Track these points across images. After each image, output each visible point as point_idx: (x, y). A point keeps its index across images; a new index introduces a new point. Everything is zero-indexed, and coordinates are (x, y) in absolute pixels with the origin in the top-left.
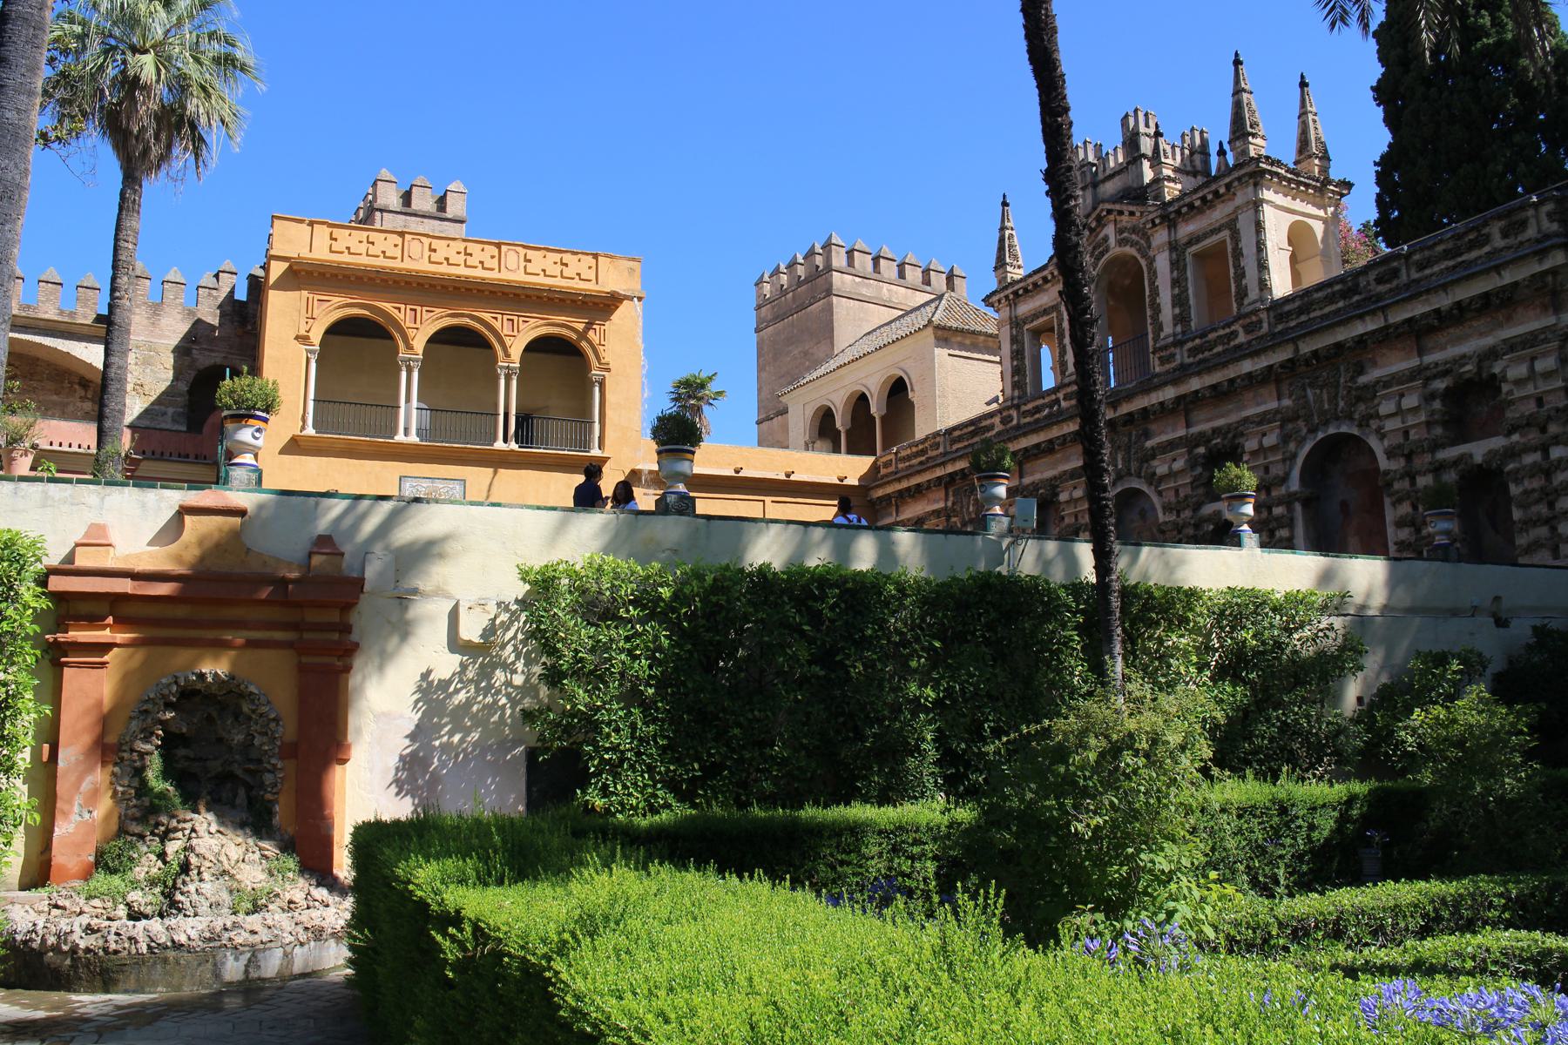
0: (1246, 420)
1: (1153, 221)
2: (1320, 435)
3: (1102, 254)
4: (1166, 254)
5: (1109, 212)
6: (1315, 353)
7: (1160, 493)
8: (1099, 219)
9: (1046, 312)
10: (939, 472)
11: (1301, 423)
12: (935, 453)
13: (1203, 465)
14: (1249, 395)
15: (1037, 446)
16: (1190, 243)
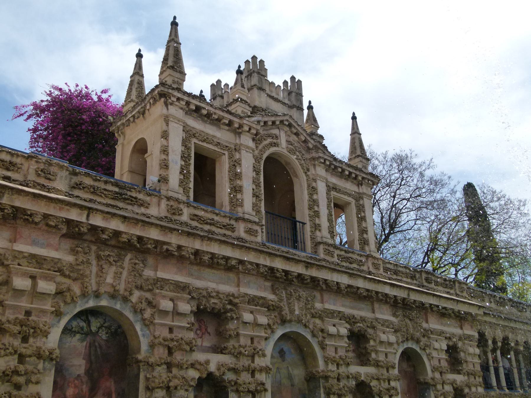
0: (377, 319)
1: (325, 160)
2: (405, 346)
3: (276, 145)
4: (324, 185)
5: (290, 126)
6: (415, 301)
7: (323, 347)
8: (282, 122)
9: (218, 144)
10: (74, 215)
11: (399, 334)
12: (42, 181)
13: (348, 337)
14: (376, 306)
15: (227, 259)
16: (335, 188)
